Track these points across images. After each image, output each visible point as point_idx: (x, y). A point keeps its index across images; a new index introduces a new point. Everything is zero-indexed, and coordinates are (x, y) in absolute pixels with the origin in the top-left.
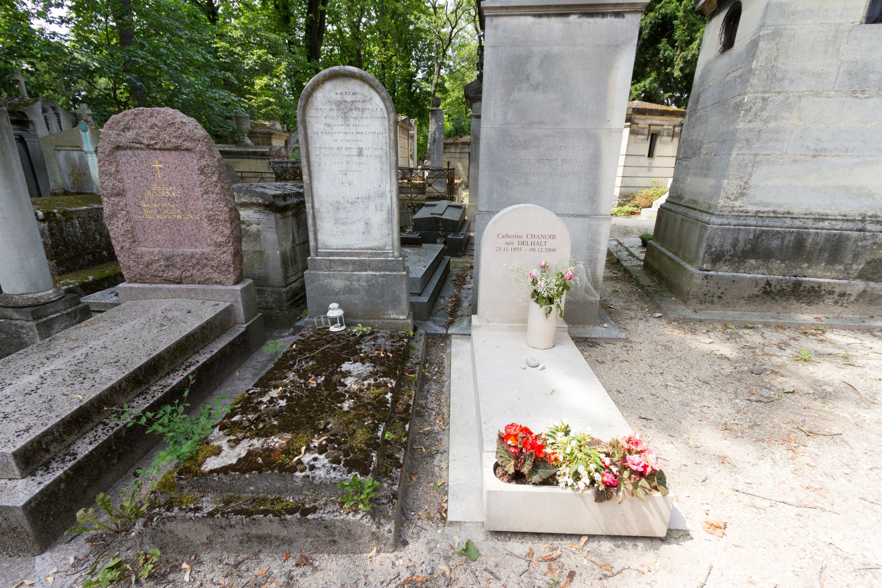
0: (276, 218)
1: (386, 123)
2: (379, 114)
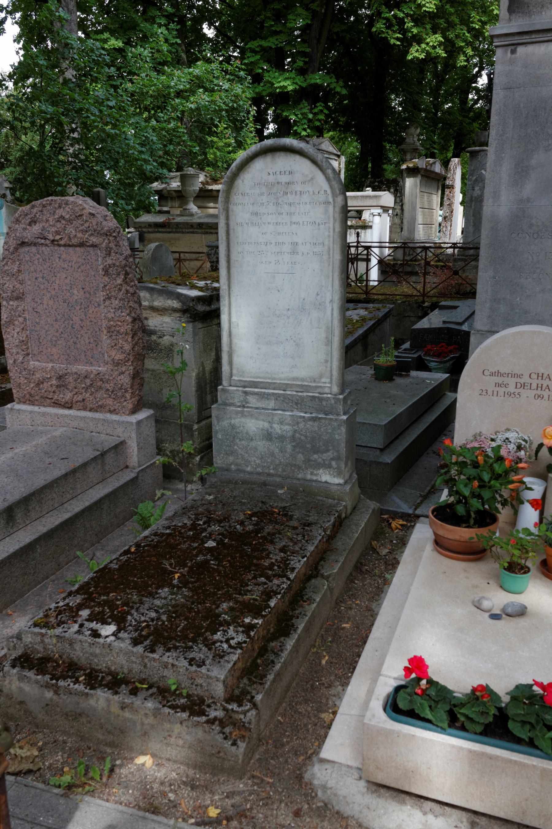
0: (194, 328)
1: (331, 208)
2: (322, 197)
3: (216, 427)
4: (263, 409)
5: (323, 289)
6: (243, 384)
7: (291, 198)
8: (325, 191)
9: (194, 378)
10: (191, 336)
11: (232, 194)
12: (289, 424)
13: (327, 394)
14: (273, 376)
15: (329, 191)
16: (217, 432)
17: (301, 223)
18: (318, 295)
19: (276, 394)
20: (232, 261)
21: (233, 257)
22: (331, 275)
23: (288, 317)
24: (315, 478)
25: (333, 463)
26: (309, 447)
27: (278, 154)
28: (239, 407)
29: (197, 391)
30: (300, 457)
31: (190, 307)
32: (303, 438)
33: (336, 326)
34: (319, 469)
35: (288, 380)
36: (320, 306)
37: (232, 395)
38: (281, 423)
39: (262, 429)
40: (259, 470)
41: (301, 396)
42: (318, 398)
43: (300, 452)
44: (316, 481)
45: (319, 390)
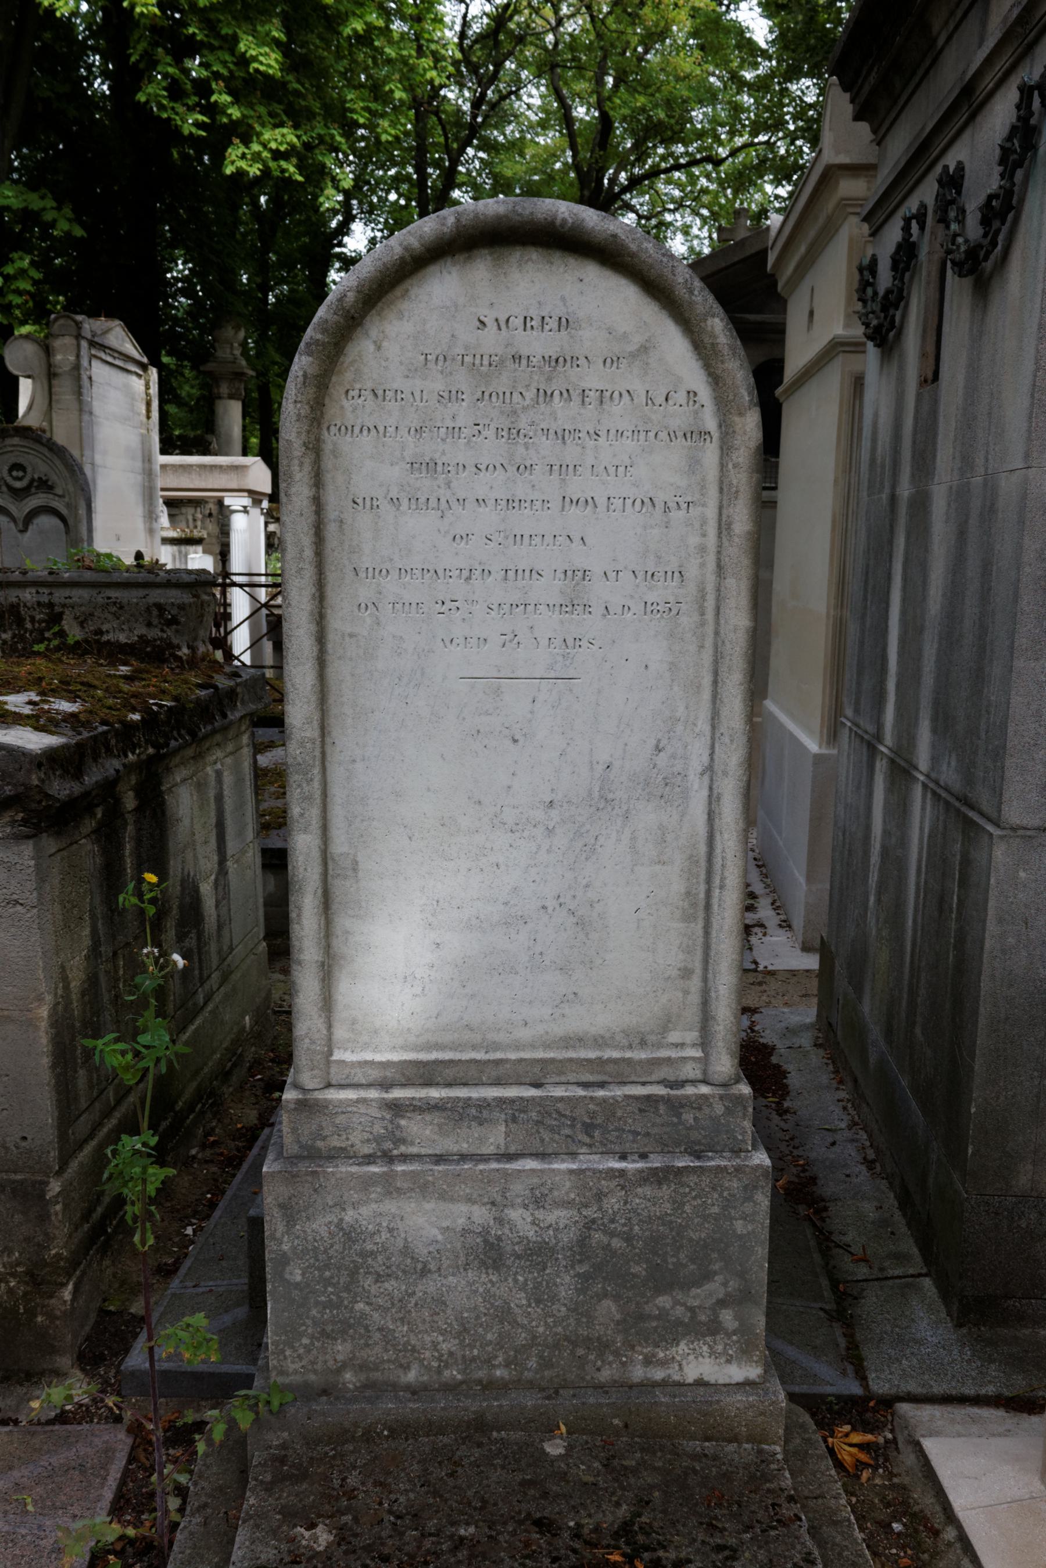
0: (38, 856)
1: (710, 454)
2: (679, 417)
3: (279, 1239)
4: (463, 1157)
5: (679, 728)
6: (375, 1074)
7: (564, 413)
8: (692, 394)
9: (44, 1025)
10: (31, 885)
11: (336, 391)
12: (567, 1204)
13: (693, 1082)
14: (493, 1036)
15: (705, 394)
16: (284, 1260)
17: (601, 501)
18: (658, 749)
19: (512, 1101)
20: (332, 638)
21: (337, 623)
22: (707, 680)
23: (550, 831)
24: (659, 1374)
25: (727, 1317)
26: (634, 1273)
27: (517, 254)
28: (369, 1159)
29: (54, 1066)
30: (608, 1309)
31: (28, 788)
32: (616, 1243)
33: (730, 855)
34: (676, 1342)
35: (547, 1046)
36: (665, 788)
37: (340, 1119)
38: (538, 1200)
39: (465, 1232)
40: (453, 1374)
41: (604, 1100)
42: (667, 1100)
43: (605, 1295)
44: (664, 1383)
45: (664, 1073)
